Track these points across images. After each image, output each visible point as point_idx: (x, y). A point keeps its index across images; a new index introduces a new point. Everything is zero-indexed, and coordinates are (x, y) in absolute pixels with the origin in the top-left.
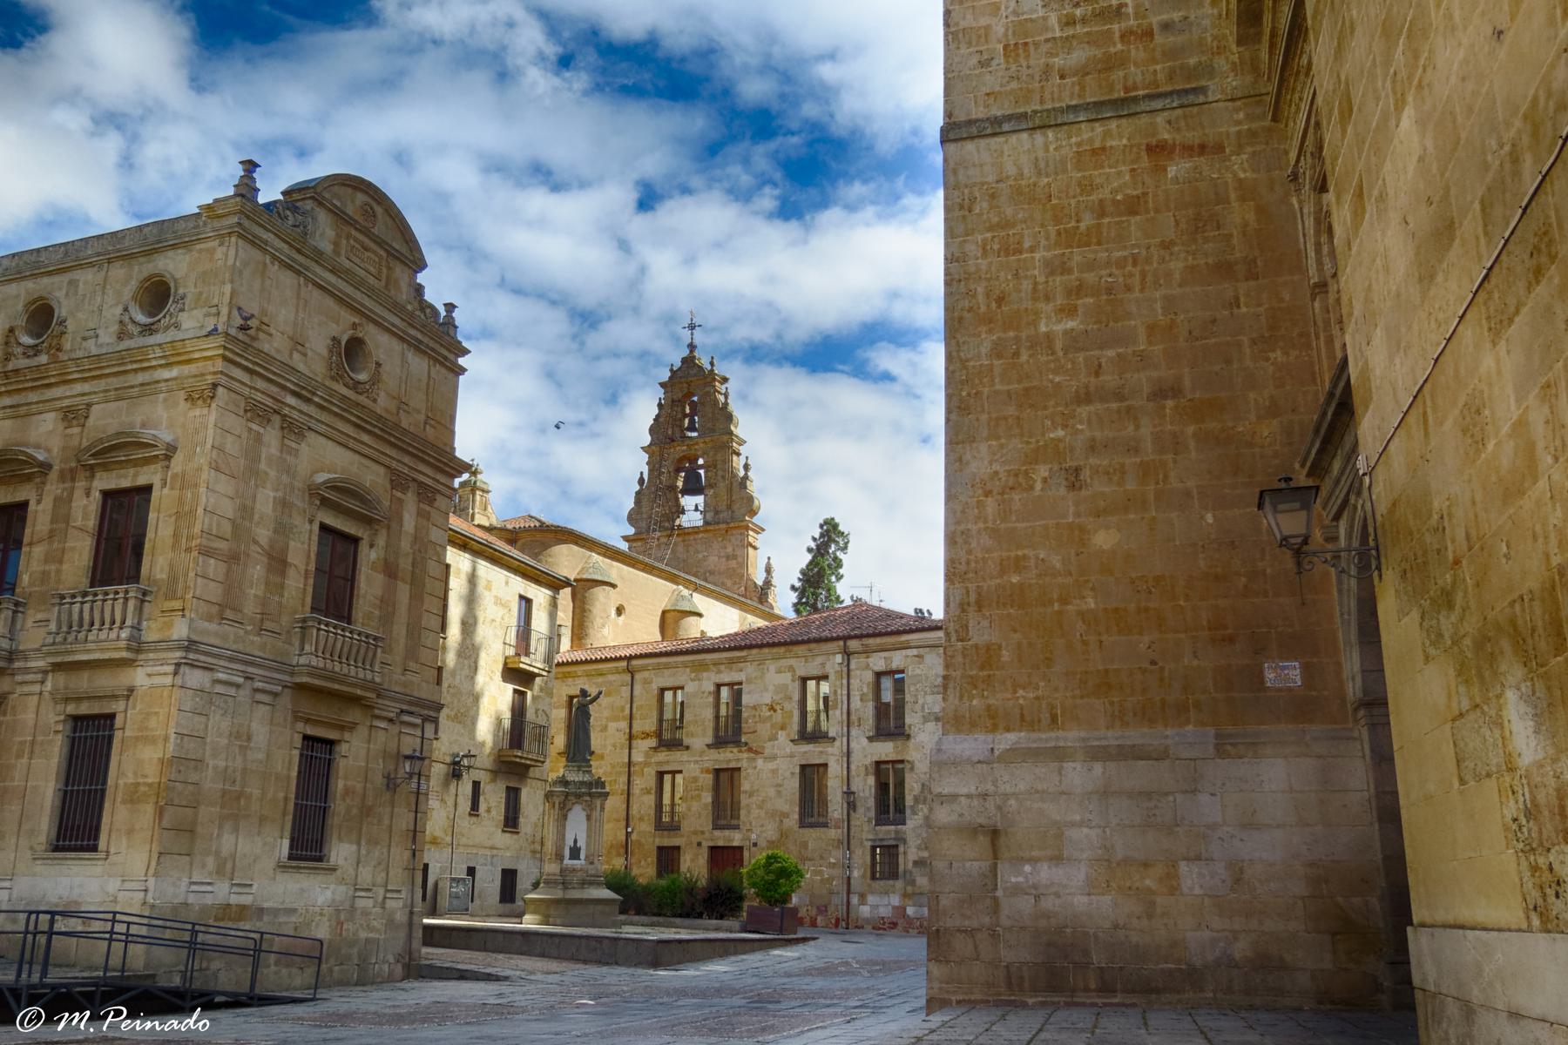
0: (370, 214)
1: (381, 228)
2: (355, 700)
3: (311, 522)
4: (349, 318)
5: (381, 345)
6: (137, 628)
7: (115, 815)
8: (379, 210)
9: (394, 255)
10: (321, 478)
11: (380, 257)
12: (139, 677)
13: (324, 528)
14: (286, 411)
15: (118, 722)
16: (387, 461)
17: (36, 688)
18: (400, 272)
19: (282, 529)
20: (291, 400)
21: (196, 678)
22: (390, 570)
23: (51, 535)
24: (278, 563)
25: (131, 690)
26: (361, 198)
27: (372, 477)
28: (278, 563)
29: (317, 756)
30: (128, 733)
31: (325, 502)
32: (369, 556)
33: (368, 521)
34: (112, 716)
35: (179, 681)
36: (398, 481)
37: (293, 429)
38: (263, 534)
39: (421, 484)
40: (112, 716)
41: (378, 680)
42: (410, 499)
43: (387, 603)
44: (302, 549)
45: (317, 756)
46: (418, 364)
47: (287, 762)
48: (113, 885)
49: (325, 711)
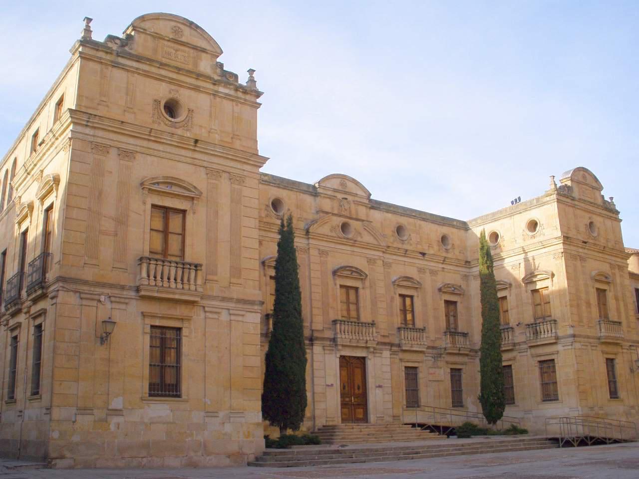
0: (584, 177)
1: (589, 180)
2: (617, 344)
3: (593, 288)
4: (587, 215)
5: (598, 220)
6: (556, 332)
7: (562, 390)
8: (586, 174)
9: (593, 188)
10: (593, 273)
11: (590, 190)
12: (559, 347)
13: (598, 289)
14: (580, 254)
15: (556, 361)
16: (608, 261)
17: (525, 354)
18: (597, 192)
19: (587, 293)
20: (581, 250)
21: (578, 345)
22: (617, 299)
23: (517, 306)
24: (588, 304)
25: (558, 352)
26: (582, 173)
27: (605, 268)
28: (588, 304)
29: (610, 362)
30: (560, 364)
31: (597, 281)
32: (610, 295)
33: (608, 283)
34: (553, 360)
35: (573, 347)
36: (612, 266)
37: (582, 259)
38: (583, 296)
39: (618, 266)
40: (553, 360)
41: (623, 336)
42: (617, 271)
43: (618, 310)
44: (593, 298)
45: (610, 362)
46: (609, 223)
47: (603, 368)
48: (567, 410)
49: (610, 349)
